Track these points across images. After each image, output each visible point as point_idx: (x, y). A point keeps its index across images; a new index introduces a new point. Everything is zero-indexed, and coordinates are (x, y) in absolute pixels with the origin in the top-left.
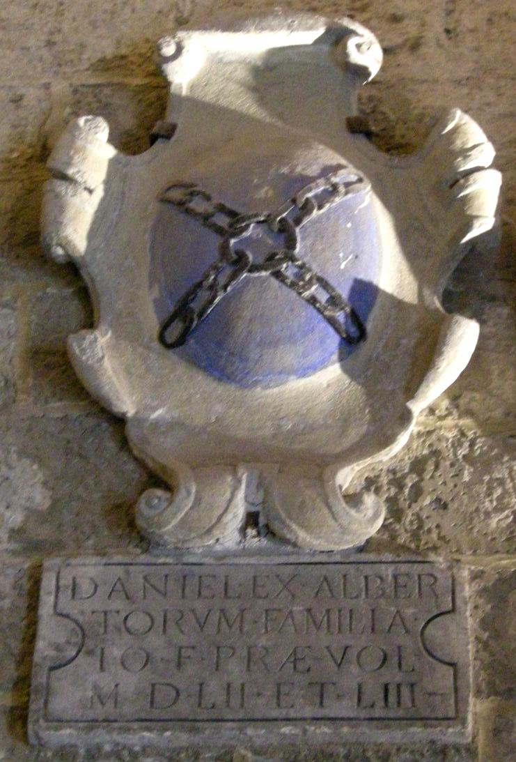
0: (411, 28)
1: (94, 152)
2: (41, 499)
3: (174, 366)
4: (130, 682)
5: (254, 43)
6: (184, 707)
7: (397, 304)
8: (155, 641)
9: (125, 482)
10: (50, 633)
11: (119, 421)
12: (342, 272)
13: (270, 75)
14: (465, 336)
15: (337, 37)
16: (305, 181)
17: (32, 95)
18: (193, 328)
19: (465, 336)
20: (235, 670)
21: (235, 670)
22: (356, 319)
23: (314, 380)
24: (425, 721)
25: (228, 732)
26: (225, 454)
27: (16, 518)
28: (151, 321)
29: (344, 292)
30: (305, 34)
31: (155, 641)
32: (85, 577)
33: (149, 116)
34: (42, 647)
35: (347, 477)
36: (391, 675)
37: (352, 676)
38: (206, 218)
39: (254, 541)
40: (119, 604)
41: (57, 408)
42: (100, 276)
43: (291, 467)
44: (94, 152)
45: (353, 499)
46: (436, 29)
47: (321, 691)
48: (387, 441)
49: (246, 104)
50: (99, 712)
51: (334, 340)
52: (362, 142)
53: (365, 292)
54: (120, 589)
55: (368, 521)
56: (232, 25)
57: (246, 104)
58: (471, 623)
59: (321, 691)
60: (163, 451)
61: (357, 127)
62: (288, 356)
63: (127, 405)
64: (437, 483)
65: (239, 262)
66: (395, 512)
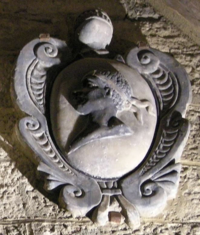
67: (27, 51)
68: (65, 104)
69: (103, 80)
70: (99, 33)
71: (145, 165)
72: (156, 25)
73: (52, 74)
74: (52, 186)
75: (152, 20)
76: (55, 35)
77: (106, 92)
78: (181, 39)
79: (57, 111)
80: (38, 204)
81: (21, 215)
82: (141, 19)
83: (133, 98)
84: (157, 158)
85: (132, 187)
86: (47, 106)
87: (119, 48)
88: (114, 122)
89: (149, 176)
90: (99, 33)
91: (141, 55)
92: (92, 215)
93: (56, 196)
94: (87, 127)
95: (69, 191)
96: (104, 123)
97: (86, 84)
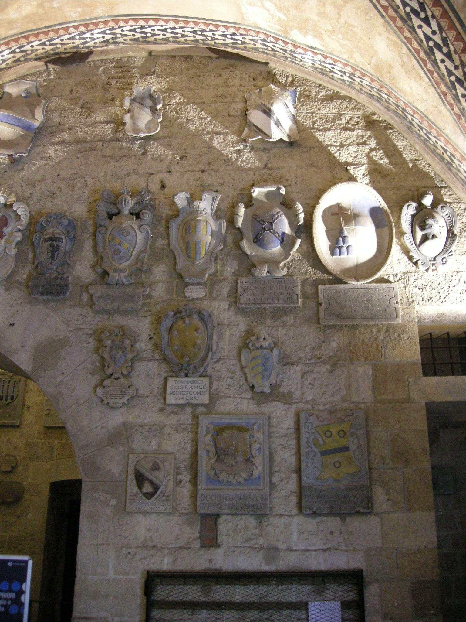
0: (290, 182)
1: (242, 210)
2: (237, 267)
3: (255, 246)
4: (251, 298)
5: (265, 190)
6: (259, 302)
7: (289, 235)
8: (255, 291)
9: (249, 265)
10: (239, 290)
11: (248, 255)
12: (280, 230)
13: (268, 195)
14: (299, 242)
15: (279, 189)
16: (274, 215)
17: (231, 195)
18: (258, 240)
19: (299, 242)
20: (266, 296)
21: (266, 296)
22: (282, 238)
23: (276, 249)
24: (293, 303)
25: (265, 305)
26: (264, 261)
27: (233, 270)
28: (252, 238)
29: (280, 234)
30: (274, 188)
31: (255, 291)
32: (244, 281)
33: (249, 203)
34: (239, 292)
35: (282, 265)
36: (289, 296)
37: (283, 297)
38: (259, 222)
39: (268, 275)
40: (249, 285)
41: (238, 252)
42: (244, 231)
43: (273, 263)
44: (242, 210)
45: (283, 269)
46: (293, 183)
47: (278, 299)
48: (287, 259)
49: (264, 200)
50: (247, 302)
51: (279, 242)
52: (283, 207)
53: (284, 234)
54: (249, 283)
55: (285, 272)
56: (262, 187)
57: (264, 200)
58: (299, 287)
59: (278, 299)
60: (255, 260)
61: (282, 204)
62: (272, 245)
63: (249, 253)
64: (295, 264)
65: (265, 230)
66: (289, 269)
67: (405, 207)
68: (418, 229)
69: (430, 221)
70: (428, 201)
71: (443, 252)
72: (446, 190)
73: (413, 216)
74: (414, 261)
75: (445, 187)
76: (414, 201)
77: (431, 226)
78: (454, 196)
79: (415, 232)
80: (410, 267)
81: (405, 270)
82: (441, 187)
83: (438, 226)
84: (446, 249)
85: (439, 259)
86: (412, 229)
87: (435, 205)
88: (434, 237)
89: (444, 256)
90: (428, 201)
91: (442, 208)
92: (427, 270)
93: (416, 263)
94: (425, 238)
95: (420, 262)
96: (430, 237)
97: (424, 222)
